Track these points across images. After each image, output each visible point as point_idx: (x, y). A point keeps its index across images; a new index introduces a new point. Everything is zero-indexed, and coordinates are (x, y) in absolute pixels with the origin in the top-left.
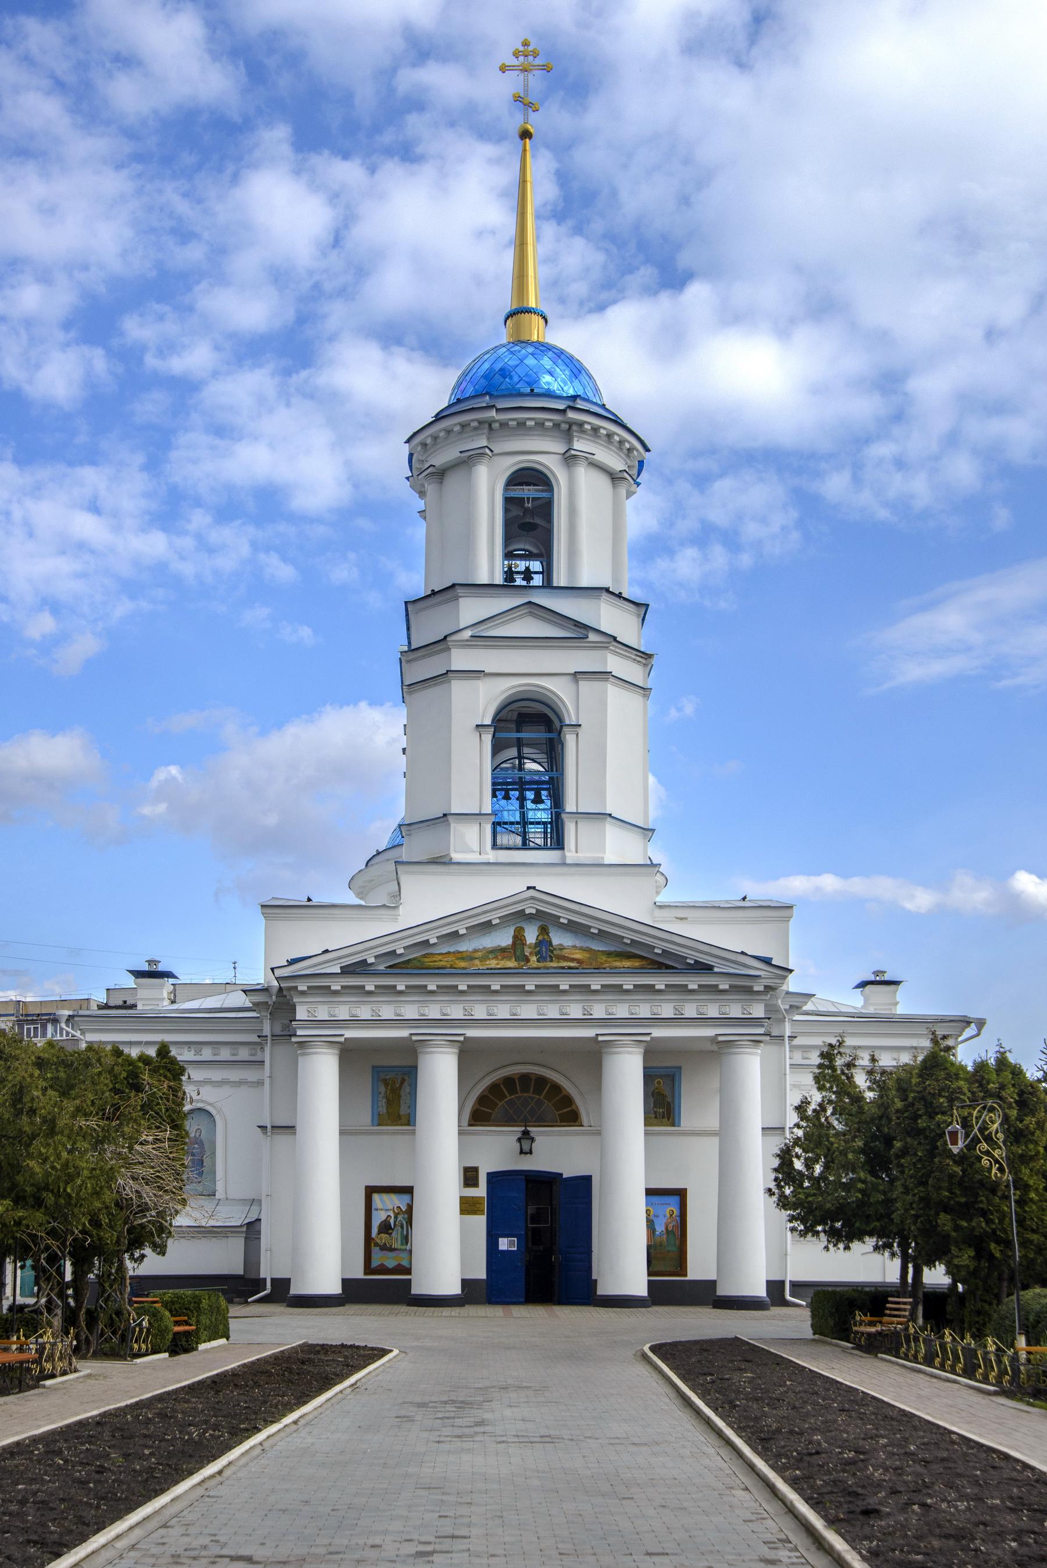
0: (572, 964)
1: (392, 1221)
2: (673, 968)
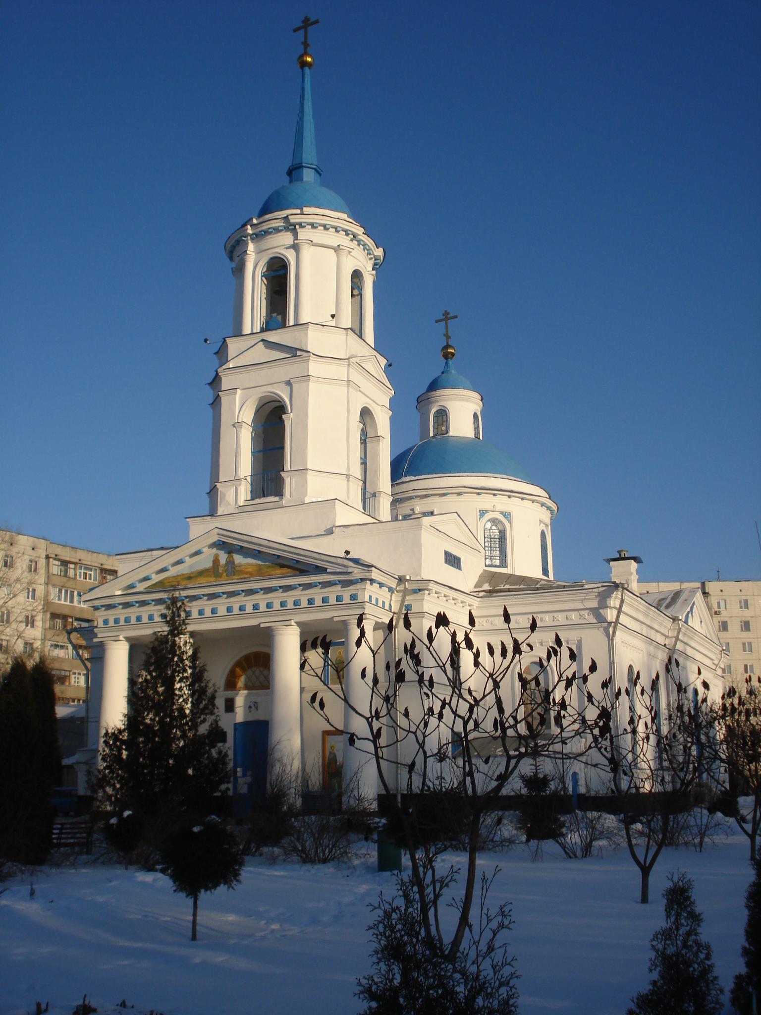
2: (307, 571)
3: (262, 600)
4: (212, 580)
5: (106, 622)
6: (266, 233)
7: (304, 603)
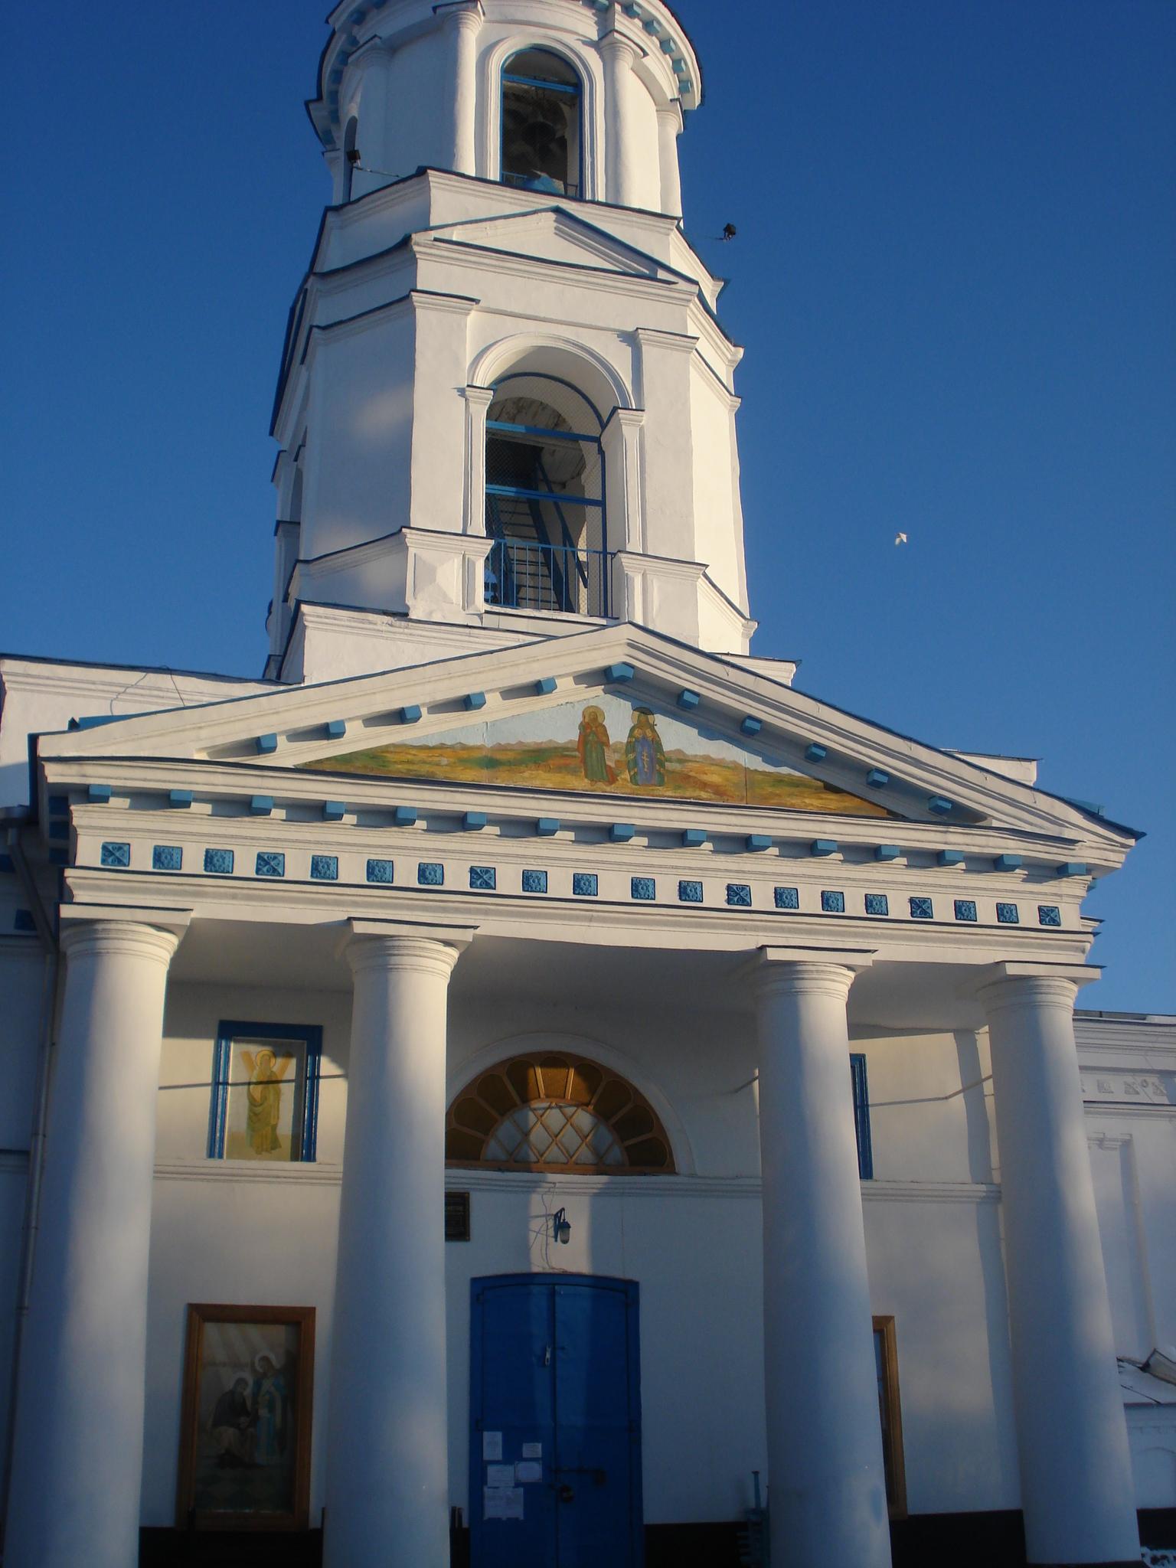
1: (248, 1392)
3: (762, 875)
4: (581, 784)
5: (115, 855)
7: (898, 908)
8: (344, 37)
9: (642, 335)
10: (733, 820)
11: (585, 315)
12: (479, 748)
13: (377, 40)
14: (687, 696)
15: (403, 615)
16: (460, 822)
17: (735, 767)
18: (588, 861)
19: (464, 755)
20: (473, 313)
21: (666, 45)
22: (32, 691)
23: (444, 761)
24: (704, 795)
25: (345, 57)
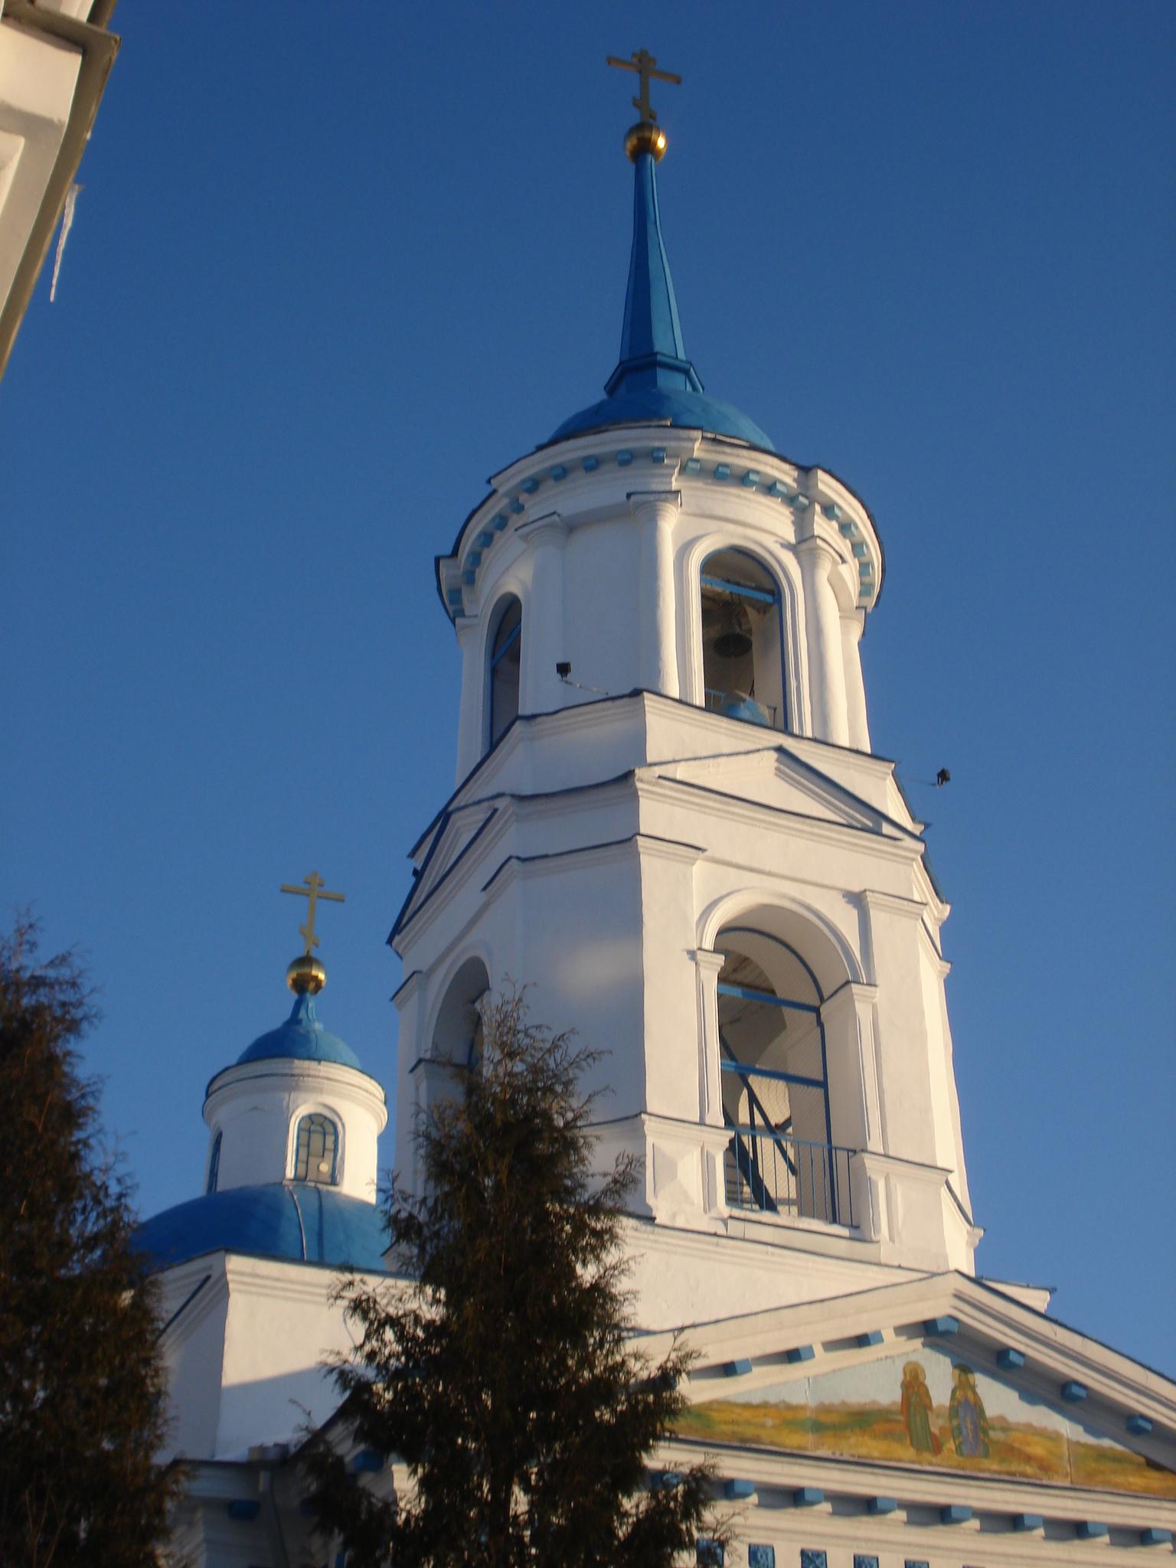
0: (1029, 1470)
4: (905, 1453)
6: (743, 479)
8: (505, 501)
9: (870, 897)
10: (1069, 1503)
11: (807, 870)
12: (803, 1408)
13: (555, 517)
14: (1013, 1357)
15: (650, 1219)
16: (795, 1497)
17: (1055, 1437)
18: (919, 1546)
19: (789, 1416)
20: (699, 862)
21: (858, 548)
22: (259, 1294)
23: (769, 1422)
24: (1029, 1470)
25: (501, 522)
